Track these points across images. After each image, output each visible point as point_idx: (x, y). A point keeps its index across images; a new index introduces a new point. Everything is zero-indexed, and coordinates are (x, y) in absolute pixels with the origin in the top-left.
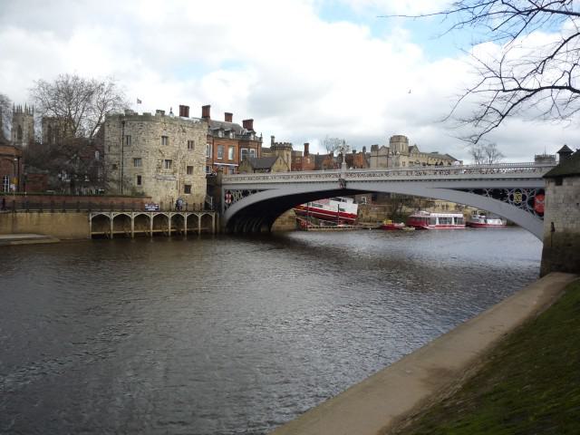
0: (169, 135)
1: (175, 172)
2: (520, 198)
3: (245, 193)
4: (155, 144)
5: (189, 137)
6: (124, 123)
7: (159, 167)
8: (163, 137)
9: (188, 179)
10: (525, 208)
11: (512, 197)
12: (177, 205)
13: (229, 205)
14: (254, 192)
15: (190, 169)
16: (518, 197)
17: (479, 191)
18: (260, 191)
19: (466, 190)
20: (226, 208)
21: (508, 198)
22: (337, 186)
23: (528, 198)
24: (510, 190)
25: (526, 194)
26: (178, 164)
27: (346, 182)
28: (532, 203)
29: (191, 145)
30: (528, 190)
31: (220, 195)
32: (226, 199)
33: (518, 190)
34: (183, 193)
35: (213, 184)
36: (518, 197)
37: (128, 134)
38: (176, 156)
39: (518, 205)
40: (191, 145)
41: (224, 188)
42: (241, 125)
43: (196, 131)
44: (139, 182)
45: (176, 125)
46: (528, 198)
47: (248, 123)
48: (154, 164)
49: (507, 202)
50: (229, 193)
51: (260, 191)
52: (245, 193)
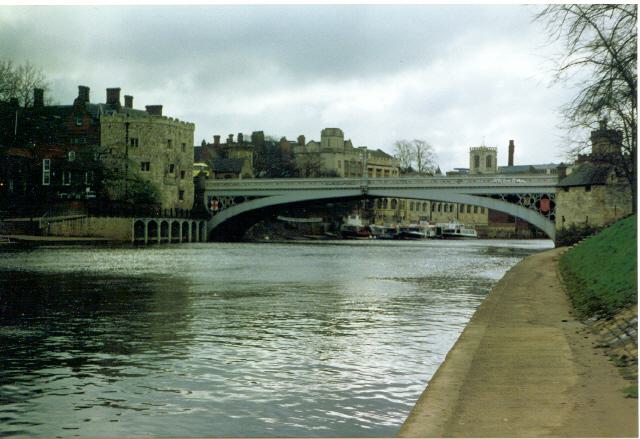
3: (239, 200)
10: (533, 209)
11: (523, 201)
13: (215, 212)
14: (251, 198)
16: (527, 202)
17: (496, 197)
19: (485, 196)
22: (358, 193)
24: (521, 195)
27: (369, 188)
28: (538, 205)
30: (535, 195)
32: (210, 205)
33: (527, 196)
36: (527, 202)
39: (527, 207)
42: (145, 109)
52: (239, 200)
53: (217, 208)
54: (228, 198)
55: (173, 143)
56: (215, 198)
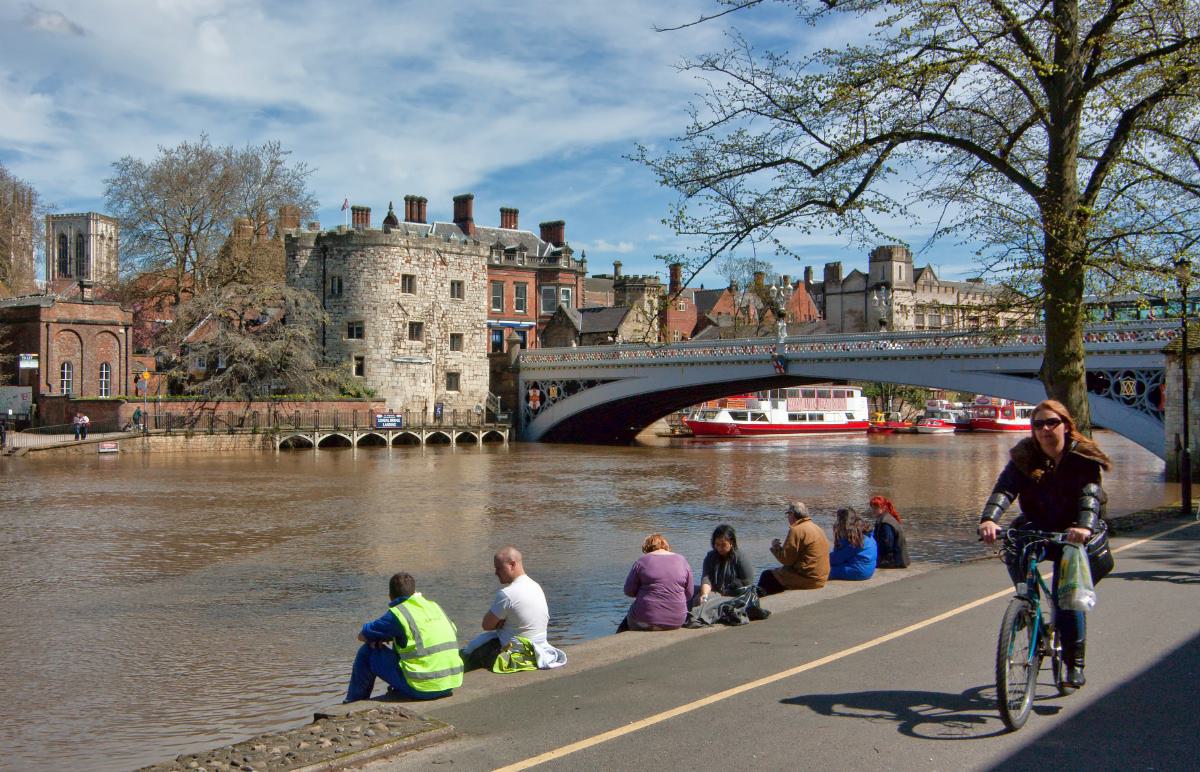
0: (417, 272)
1: (429, 347)
2: (1133, 388)
3: (572, 387)
4: (391, 291)
5: (454, 275)
6: (325, 250)
7: (399, 339)
8: (405, 277)
9: (455, 360)
10: (1143, 407)
11: (1117, 388)
12: (438, 417)
13: (536, 412)
14: (591, 384)
15: (456, 341)
18: (604, 382)
20: (528, 419)
21: (1111, 390)
22: (769, 371)
23: (1148, 388)
24: (1113, 373)
25: (1144, 381)
26: (433, 331)
29: (457, 289)
31: (516, 392)
33: (1129, 374)
34: (443, 390)
35: (502, 370)
36: (1129, 388)
37: (337, 272)
38: (429, 313)
39: (1129, 402)
40: (457, 289)
41: (526, 376)
42: (537, 234)
43: (467, 261)
44: (360, 370)
45: (428, 250)
46: (1148, 388)
47: (552, 231)
48: (388, 334)
49: (1109, 397)
50: (535, 386)
51: (604, 382)
52: (572, 387)
53: (538, 404)
54: (554, 383)
55: (419, 283)
56: (535, 386)
